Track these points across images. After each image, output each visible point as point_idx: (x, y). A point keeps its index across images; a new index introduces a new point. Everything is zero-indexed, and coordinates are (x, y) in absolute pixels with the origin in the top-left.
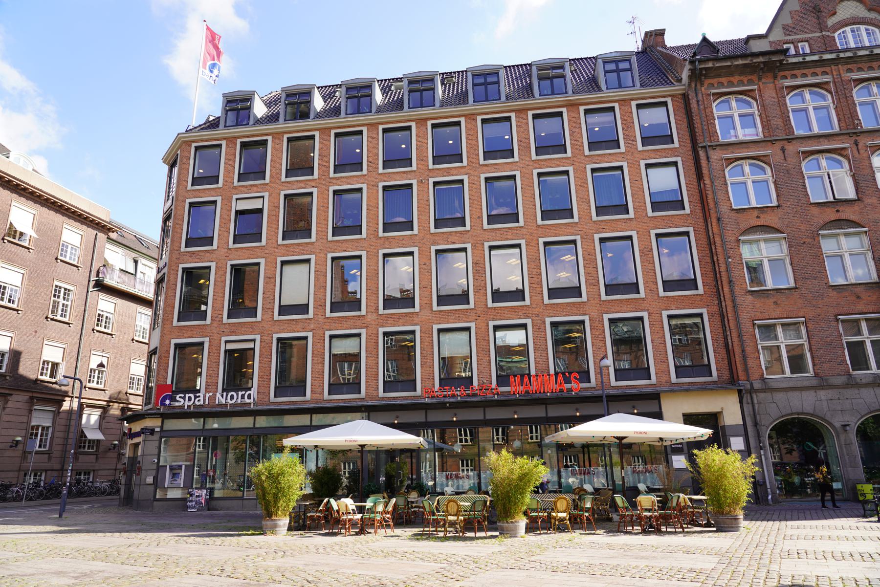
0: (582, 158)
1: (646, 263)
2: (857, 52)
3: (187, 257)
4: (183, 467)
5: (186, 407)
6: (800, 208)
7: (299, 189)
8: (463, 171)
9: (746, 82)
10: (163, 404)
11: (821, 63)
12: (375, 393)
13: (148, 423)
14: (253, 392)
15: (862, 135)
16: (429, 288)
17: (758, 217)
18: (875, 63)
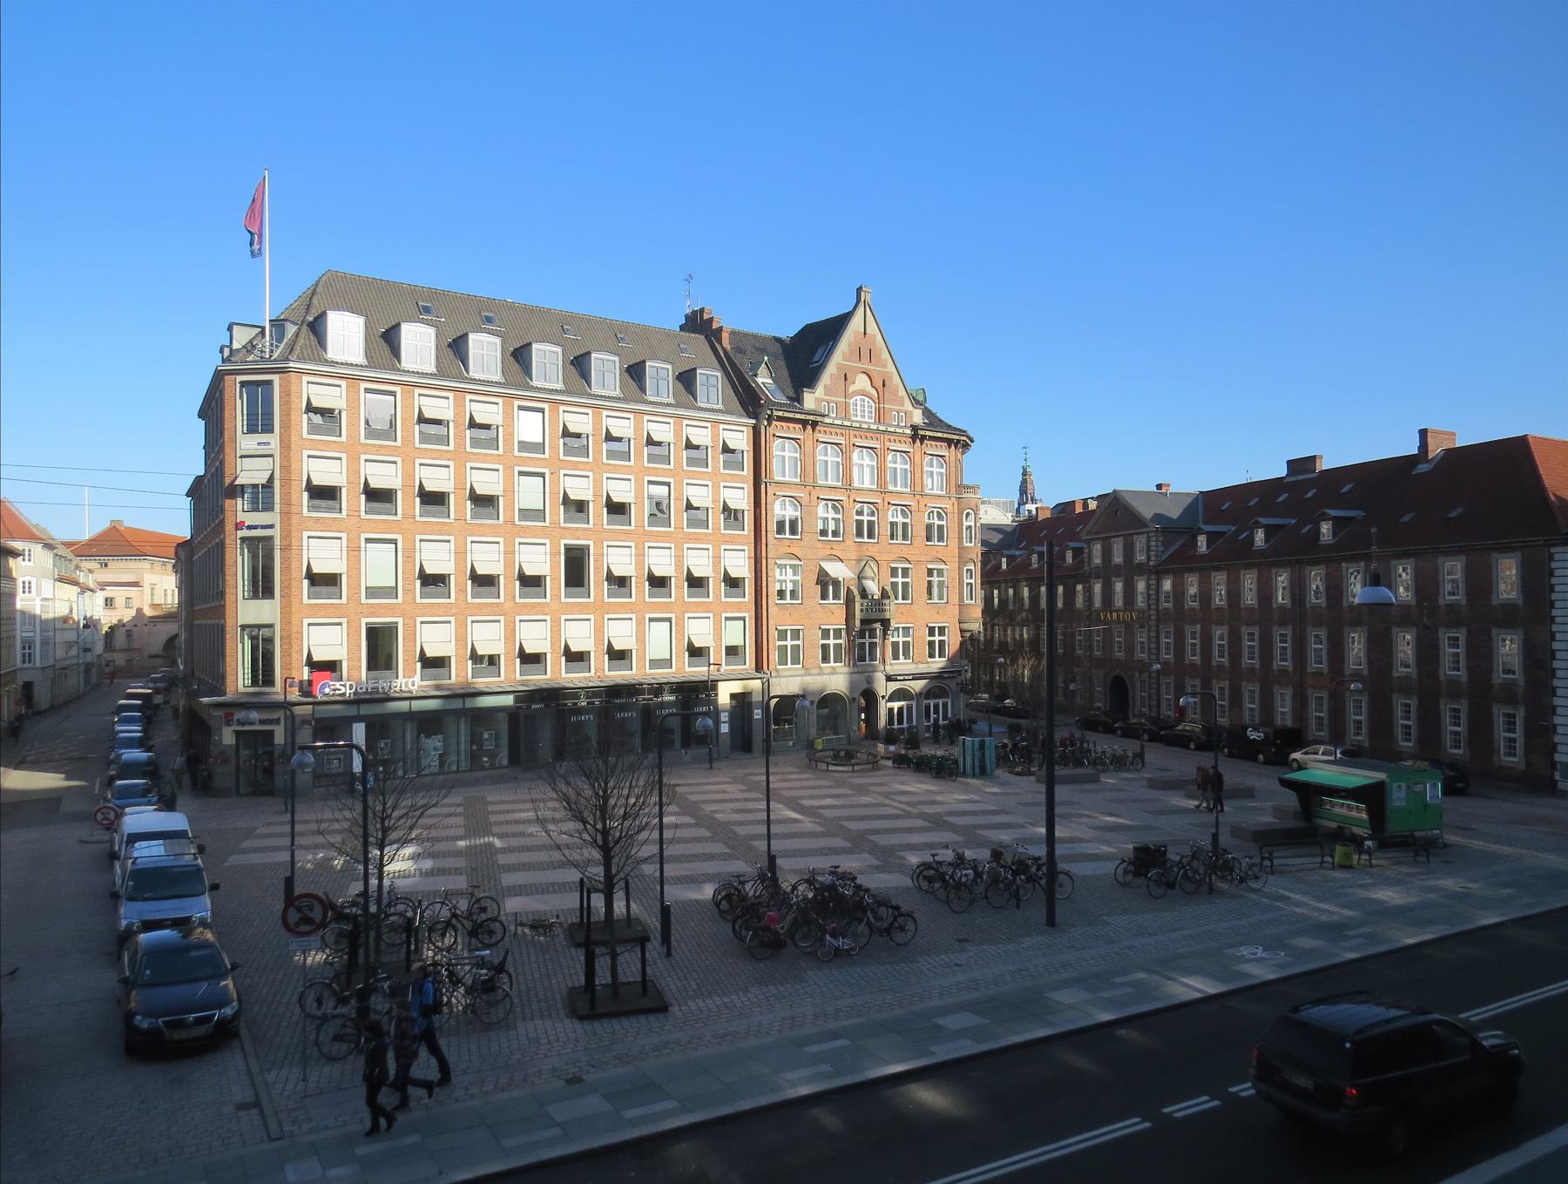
7: (435, 459)
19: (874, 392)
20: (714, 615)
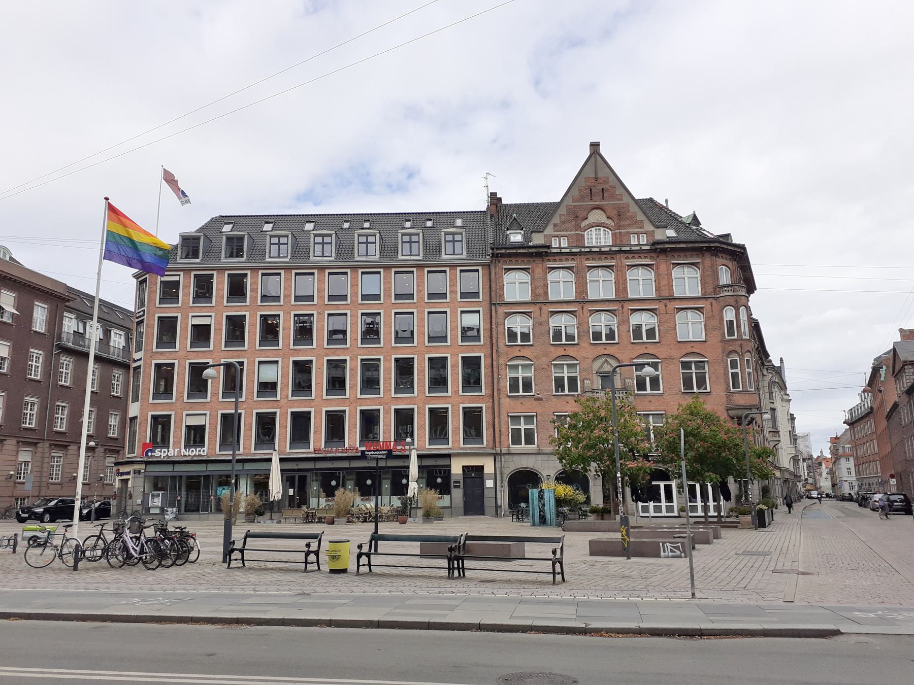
0: (423, 304)
1: (454, 375)
3: (157, 355)
4: (161, 494)
5: (162, 457)
8: (347, 307)
9: (526, 262)
10: (147, 455)
11: (571, 253)
12: (284, 450)
13: (137, 467)
14: (206, 449)
15: (587, 303)
16: (321, 384)
17: (520, 351)
18: (603, 256)
19: (609, 222)
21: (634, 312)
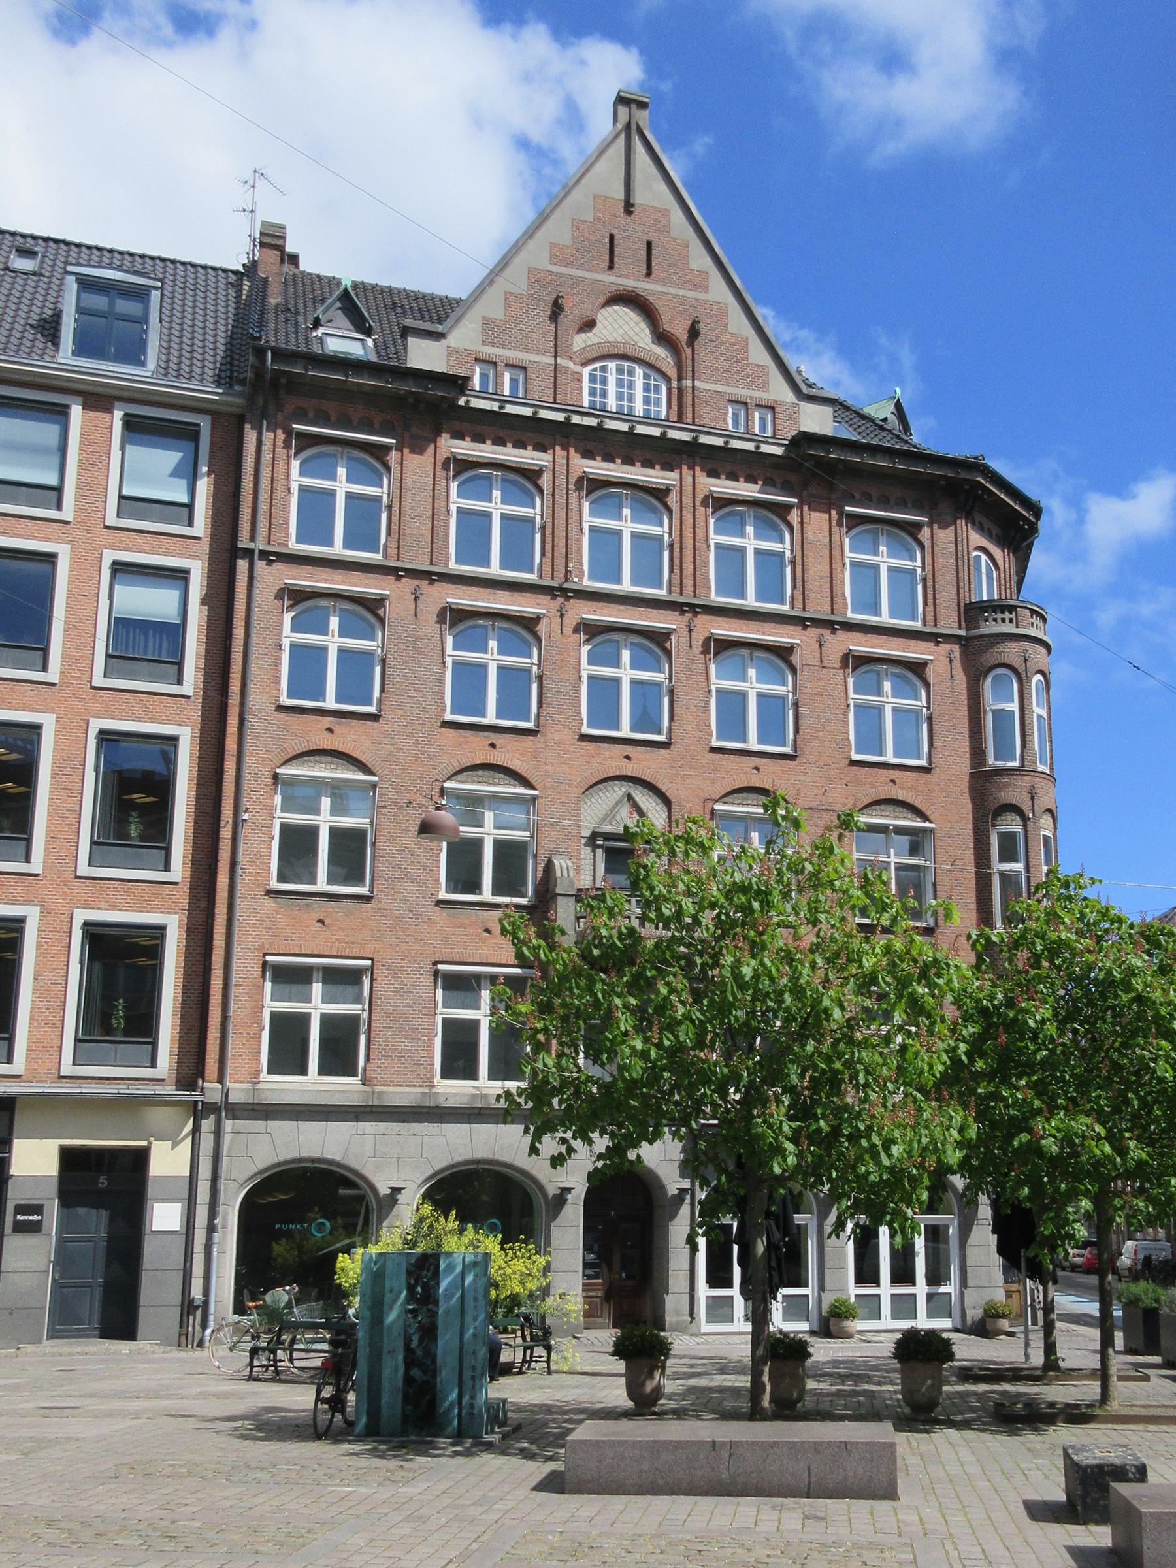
1: (63, 795)
2: (607, 420)
6: (420, 727)
9: (377, 426)
20: (44, 914)
21: (726, 649)
